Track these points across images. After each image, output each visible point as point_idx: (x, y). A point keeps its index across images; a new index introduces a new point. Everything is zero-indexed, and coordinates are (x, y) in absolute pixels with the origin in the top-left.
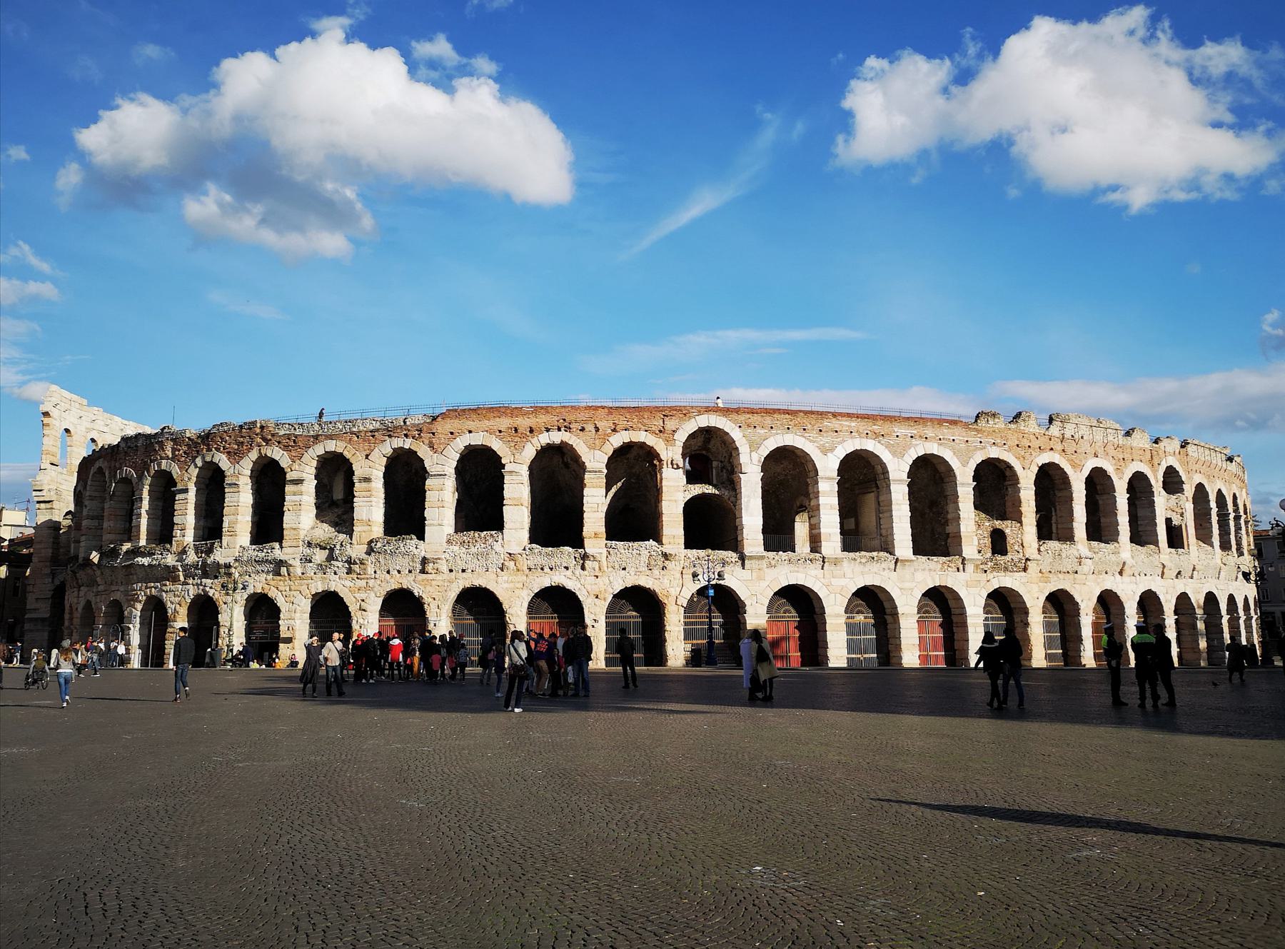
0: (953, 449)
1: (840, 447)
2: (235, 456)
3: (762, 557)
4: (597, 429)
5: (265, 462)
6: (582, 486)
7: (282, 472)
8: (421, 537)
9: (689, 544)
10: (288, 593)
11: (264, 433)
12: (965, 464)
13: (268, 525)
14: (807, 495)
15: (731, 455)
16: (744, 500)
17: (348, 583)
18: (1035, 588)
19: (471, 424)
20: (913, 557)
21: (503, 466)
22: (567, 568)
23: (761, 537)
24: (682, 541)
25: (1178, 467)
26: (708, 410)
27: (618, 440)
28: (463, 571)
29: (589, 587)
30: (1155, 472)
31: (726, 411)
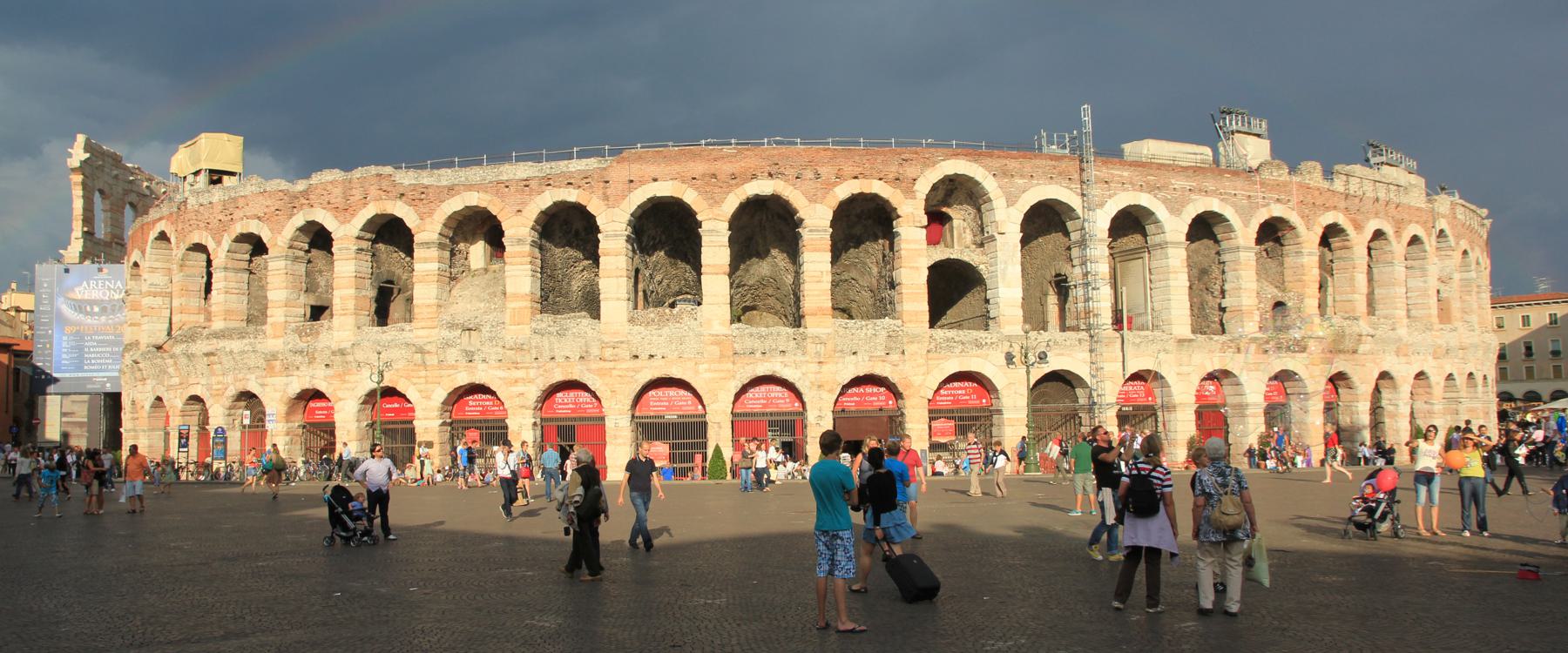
0: (1234, 205)
4: (818, 176)
8: (596, 315)
10: (422, 387)
12: (1246, 224)
13: (386, 302)
16: (1000, 267)
17: (500, 373)
18: (1317, 371)
21: (699, 224)
25: (1448, 232)
27: (844, 191)
29: (812, 377)
30: (1429, 235)
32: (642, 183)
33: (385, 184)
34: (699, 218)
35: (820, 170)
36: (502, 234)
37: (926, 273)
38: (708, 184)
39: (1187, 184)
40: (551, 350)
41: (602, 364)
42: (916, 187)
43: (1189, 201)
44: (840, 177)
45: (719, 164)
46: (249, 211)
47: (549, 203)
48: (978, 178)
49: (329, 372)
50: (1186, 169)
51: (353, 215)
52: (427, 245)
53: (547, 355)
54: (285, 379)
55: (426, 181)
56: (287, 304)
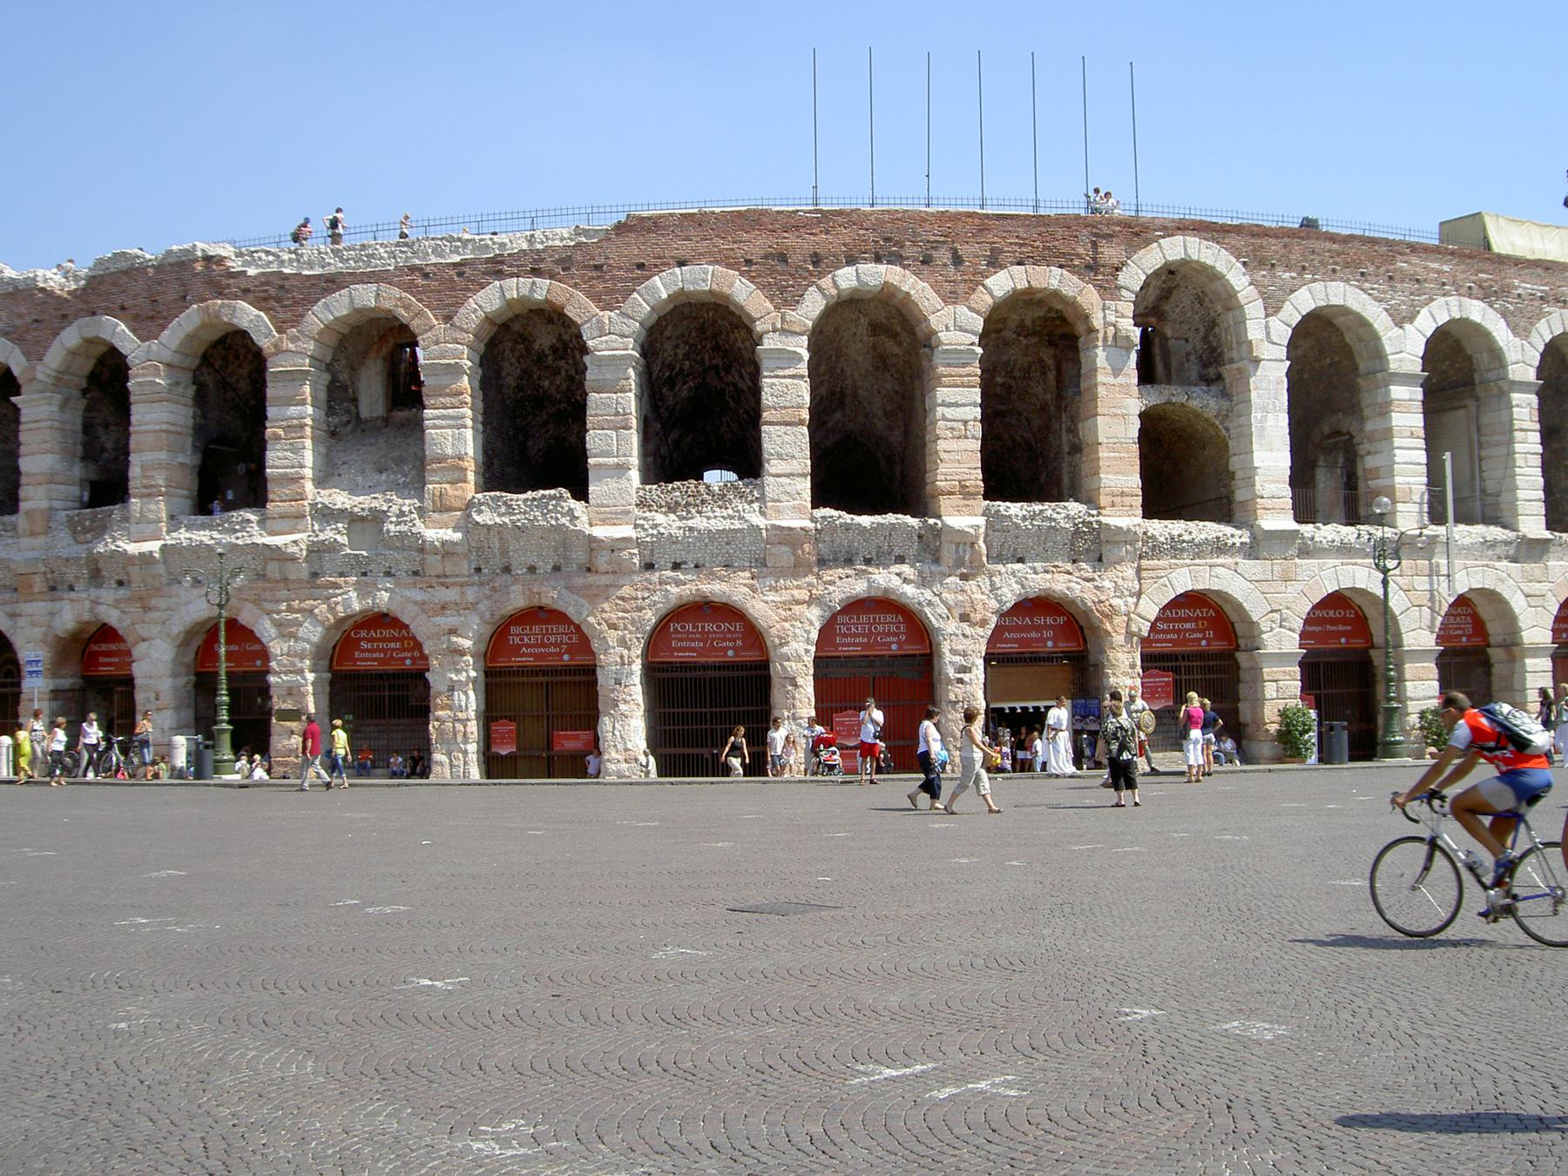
1: (1424, 311)
2: (148, 322)
4: (957, 260)
5: (215, 335)
7: (257, 360)
8: (581, 493)
11: (212, 277)
14: (1354, 408)
15: (1213, 325)
16: (1256, 415)
17: (418, 596)
20: (1548, 535)
21: (758, 341)
22: (901, 560)
23: (1288, 492)
27: (1002, 283)
28: (676, 566)
32: (658, 268)
34: (759, 327)
35: (963, 249)
37: (1136, 424)
38: (773, 272)
40: (504, 553)
41: (591, 578)
42: (1123, 279)
43: (1540, 315)
44: (995, 263)
45: (790, 240)
48: (1220, 267)
49: (122, 592)
50: (1537, 263)
51: (163, 328)
53: (498, 562)
54: (50, 605)
56: (51, 479)
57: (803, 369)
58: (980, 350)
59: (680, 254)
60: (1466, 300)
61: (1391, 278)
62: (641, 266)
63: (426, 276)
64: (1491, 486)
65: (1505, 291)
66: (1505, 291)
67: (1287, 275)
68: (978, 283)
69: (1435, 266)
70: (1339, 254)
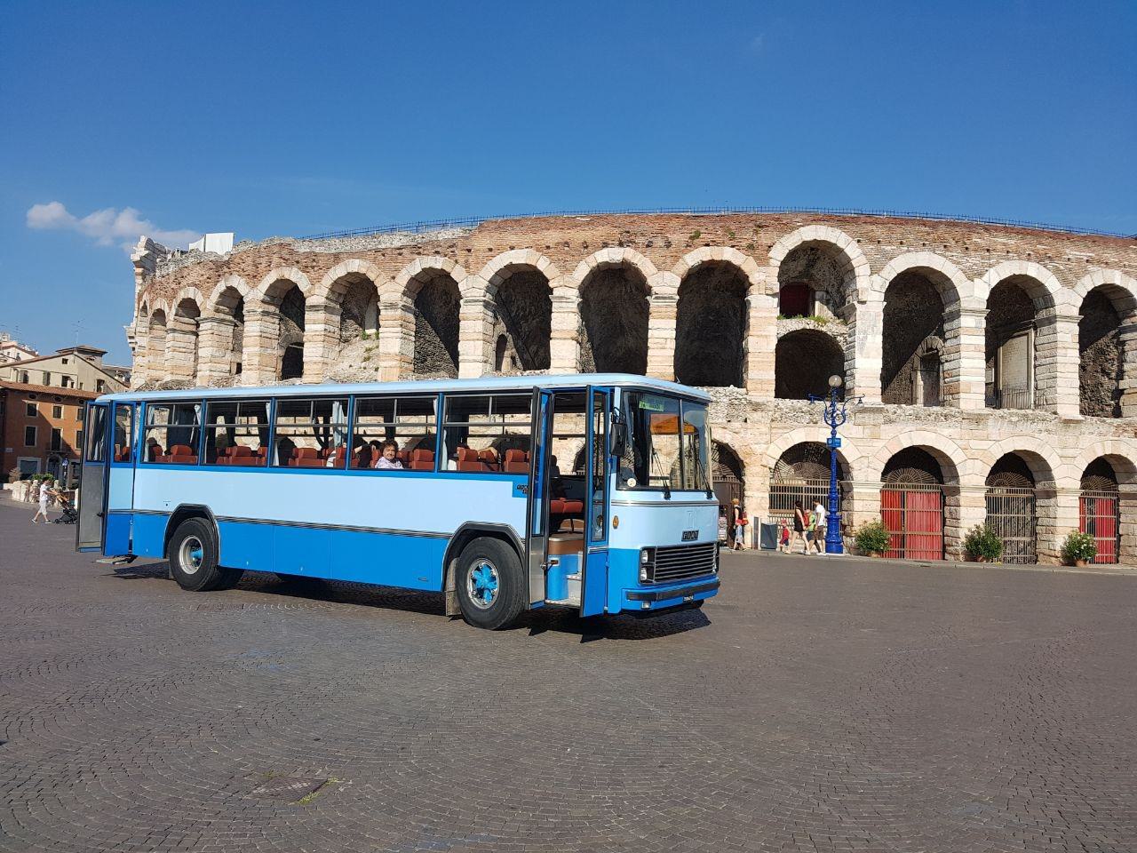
3: (880, 410)
4: (668, 245)
6: (644, 313)
9: (780, 393)
16: (858, 336)
19: (512, 239)
20: (1080, 417)
21: (551, 291)
24: (774, 387)
26: (817, 220)
27: (695, 257)
31: (840, 221)
32: (501, 250)
33: (285, 253)
34: (551, 284)
36: (377, 298)
39: (1085, 255)
43: (1086, 272)
46: (191, 279)
47: (419, 270)
48: (841, 245)
52: (315, 308)
55: (317, 250)
57: (574, 307)
58: (678, 297)
59: (513, 243)
60: (1025, 263)
61: (967, 248)
62: (491, 250)
63: (384, 255)
64: (1041, 384)
65: (1059, 256)
66: (1059, 256)
67: (889, 248)
68: (680, 257)
69: (1000, 240)
70: (929, 234)
